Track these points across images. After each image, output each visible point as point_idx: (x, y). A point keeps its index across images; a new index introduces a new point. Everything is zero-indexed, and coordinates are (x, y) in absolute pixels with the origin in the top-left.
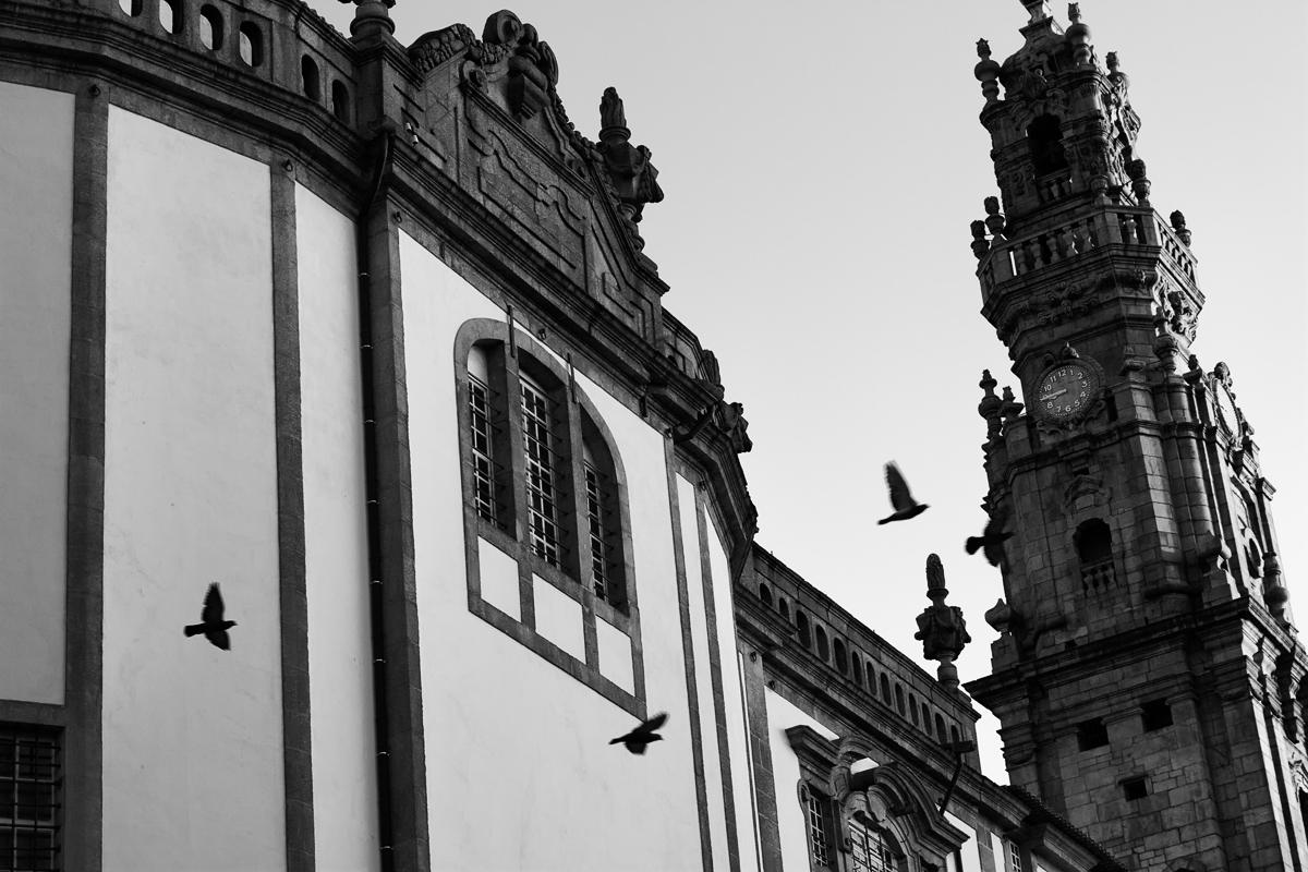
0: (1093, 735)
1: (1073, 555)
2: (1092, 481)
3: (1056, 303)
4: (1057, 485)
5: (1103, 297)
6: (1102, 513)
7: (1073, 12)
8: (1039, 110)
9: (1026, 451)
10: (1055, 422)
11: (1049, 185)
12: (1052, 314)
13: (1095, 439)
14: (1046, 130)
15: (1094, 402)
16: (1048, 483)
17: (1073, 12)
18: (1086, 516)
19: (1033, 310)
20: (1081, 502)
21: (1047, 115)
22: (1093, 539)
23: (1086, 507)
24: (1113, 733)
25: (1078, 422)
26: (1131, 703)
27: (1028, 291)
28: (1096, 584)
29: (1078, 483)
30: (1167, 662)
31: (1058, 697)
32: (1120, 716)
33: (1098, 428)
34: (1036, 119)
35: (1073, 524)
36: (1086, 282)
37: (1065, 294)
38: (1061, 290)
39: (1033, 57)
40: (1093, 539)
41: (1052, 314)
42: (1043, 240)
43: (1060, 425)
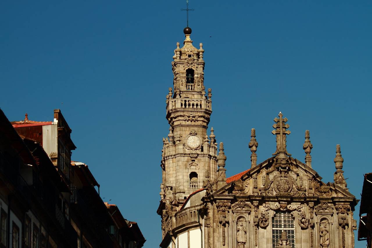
2: (196, 164)
3: (189, 117)
4: (188, 161)
6: (196, 171)
8: (190, 67)
9: (181, 151)
10: (190, 147)
11: (189, 86)
12: (187, 118)
13: (198, 155)
14: (190, 72)
16: (186, 160)
21: (192, 69)
22: (194, 175)
23: (193, 169)
27: (183, 111)
28: (192, 186)
29: (193, 163)
33: (199, 152)
34: (189, 69)
35: (190, 171)
36: (197, 115)
37: (192, 115)
38: (191, 114)
39: (190, 52)
41: (187, 118)
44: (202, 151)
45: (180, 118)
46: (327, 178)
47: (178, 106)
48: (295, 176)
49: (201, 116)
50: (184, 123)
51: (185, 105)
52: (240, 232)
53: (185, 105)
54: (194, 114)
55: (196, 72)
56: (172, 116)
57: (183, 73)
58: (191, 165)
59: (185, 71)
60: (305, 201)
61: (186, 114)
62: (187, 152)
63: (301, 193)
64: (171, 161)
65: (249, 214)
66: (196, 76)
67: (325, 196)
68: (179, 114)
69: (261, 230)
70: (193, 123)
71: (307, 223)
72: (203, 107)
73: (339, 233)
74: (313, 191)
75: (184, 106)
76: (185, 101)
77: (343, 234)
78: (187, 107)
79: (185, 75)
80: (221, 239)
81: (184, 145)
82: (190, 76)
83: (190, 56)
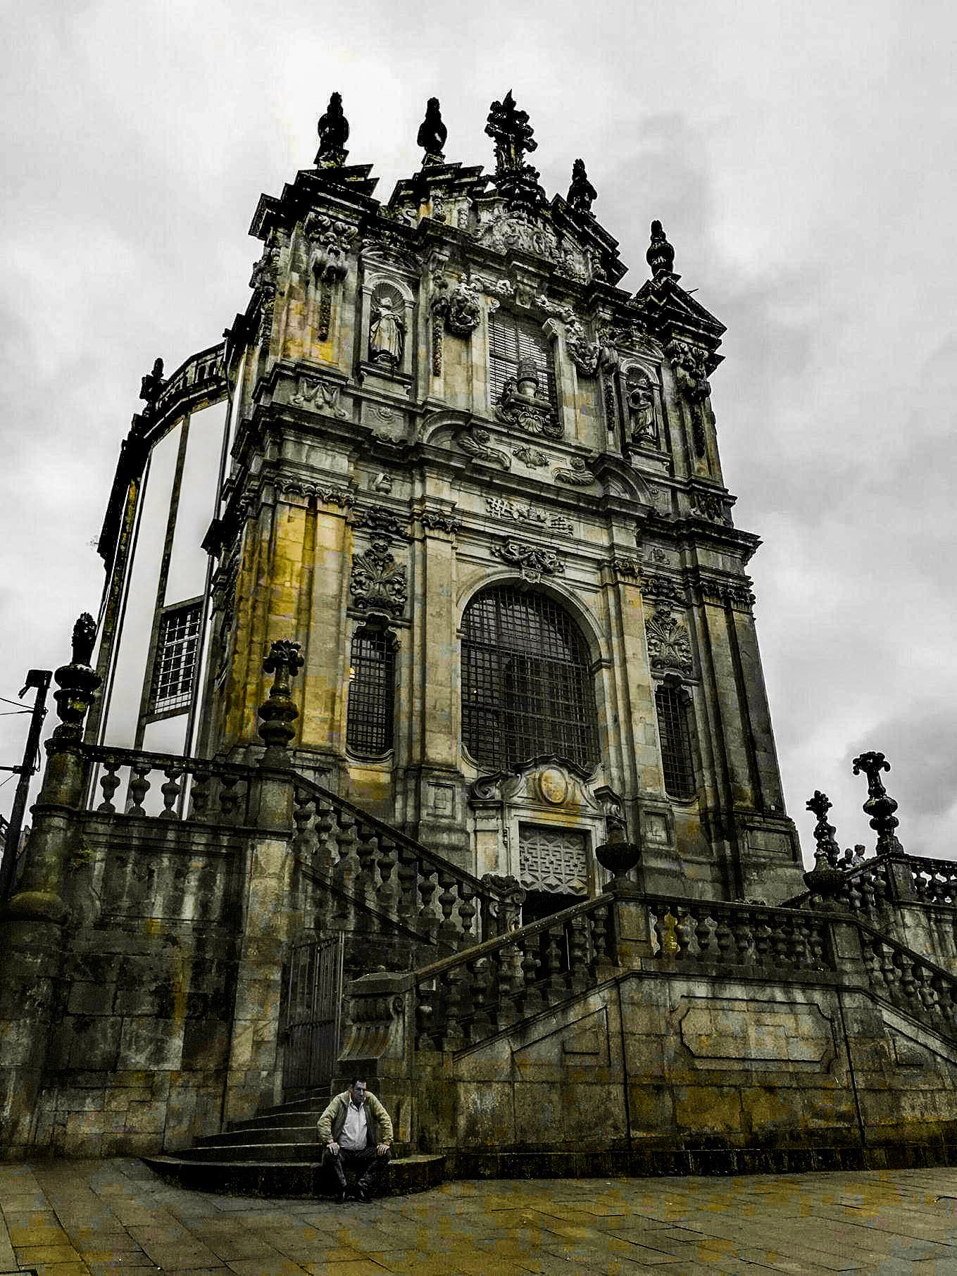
52: (384, 323)
69: (449, 346)
71: (595, 361)
73: (681, 418)
80: (314, 320)
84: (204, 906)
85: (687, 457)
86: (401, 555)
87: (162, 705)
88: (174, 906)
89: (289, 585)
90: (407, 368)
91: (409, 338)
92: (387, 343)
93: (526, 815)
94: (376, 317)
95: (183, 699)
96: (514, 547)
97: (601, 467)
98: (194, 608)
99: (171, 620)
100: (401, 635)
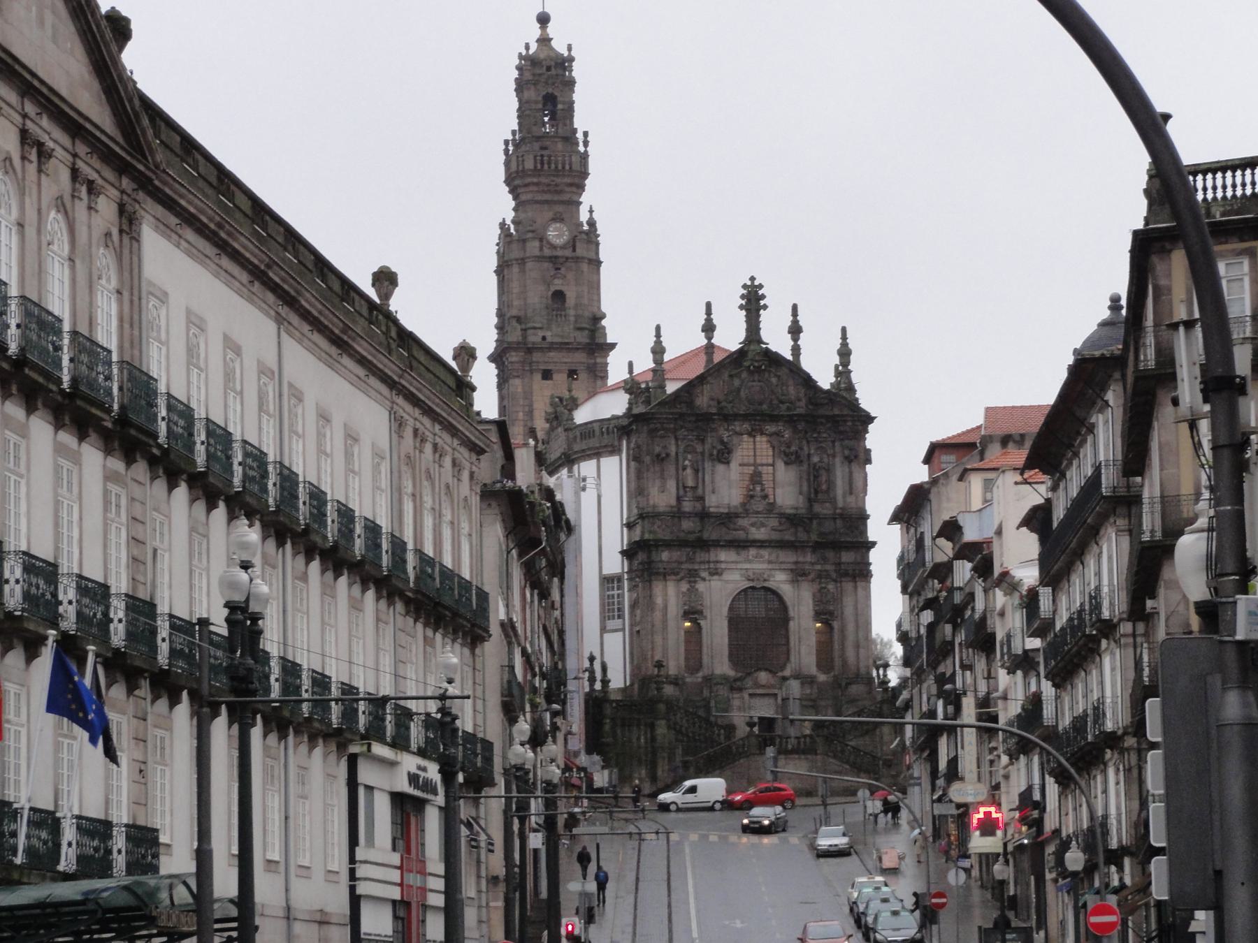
0: (547, 375)
1: (550, 301)
5: (568, 189)
7: (570, 48)
8: (550, 90)
9: (537, 253)
14: (550, 100)
15: (568, 243)
17: (570, 48)
18: (558, 288)
19: (537, 184)
20: (556, 281)
23: (558, 285)
24: (555, 376)
25: (563, 247)
26: (566, 368)
30: (580, 357)
31: (537, 356)
32: (559, 371)
33: (568, 253)
35: (553, 289)
40: (559, 296)
42: (550, 156)
43: (554, 247)
44: (574, 250)
45: (531, 188)
46: (825, 379)
47: (529, 165)
48: (774, 380)
49: (571, 185)
50: (539, 197)
51: (542, 164)
53: (542, 164)
54: (558, 180)
55: (560, 99)
56: (517, 182)
57: (536, 102)
58: (554, 277)
59: (540, 98)
60: (791, 420)
61: (543, 180)
62: (547, 252)
63: (784, 407)
64: (515, 269)
65: (703, 441)
66: (560, 106)
67: (822, 411)
68: (529, 180)
69: (721, 468)
70: (556, 198)
72: (574, 167)
74: (803, 403)
75: (539, 166)
76: (542, 156)
77: (851, 473)
78: (546, 166)
79: (540, 106)
81: (541, 240)
82: (549, 106)
83: (549, 69)
84: (646, 738)
85: (844, 497)
86: (701, 586)
87: (612, 624)
88: (638, 739)
89: (658, 615)
90: (700, 491)
91: (700, 474)
92: (690, 483)
93: (751, 691)
94: (684, 469)
95: (616, 623)
96: (750, 573)
97: (792, 520)
98: (619, 578)
99: (608, 581)
100: (702, 623)
